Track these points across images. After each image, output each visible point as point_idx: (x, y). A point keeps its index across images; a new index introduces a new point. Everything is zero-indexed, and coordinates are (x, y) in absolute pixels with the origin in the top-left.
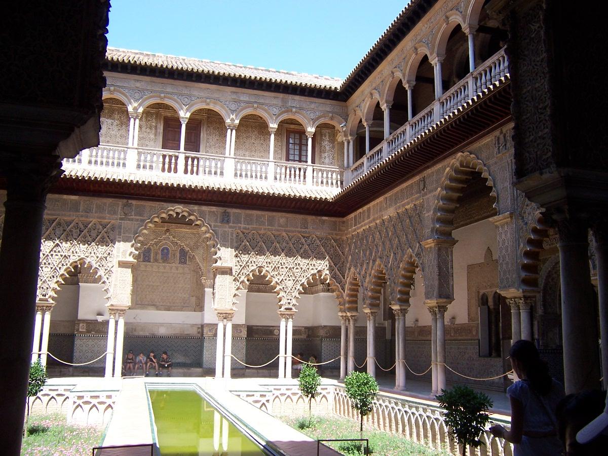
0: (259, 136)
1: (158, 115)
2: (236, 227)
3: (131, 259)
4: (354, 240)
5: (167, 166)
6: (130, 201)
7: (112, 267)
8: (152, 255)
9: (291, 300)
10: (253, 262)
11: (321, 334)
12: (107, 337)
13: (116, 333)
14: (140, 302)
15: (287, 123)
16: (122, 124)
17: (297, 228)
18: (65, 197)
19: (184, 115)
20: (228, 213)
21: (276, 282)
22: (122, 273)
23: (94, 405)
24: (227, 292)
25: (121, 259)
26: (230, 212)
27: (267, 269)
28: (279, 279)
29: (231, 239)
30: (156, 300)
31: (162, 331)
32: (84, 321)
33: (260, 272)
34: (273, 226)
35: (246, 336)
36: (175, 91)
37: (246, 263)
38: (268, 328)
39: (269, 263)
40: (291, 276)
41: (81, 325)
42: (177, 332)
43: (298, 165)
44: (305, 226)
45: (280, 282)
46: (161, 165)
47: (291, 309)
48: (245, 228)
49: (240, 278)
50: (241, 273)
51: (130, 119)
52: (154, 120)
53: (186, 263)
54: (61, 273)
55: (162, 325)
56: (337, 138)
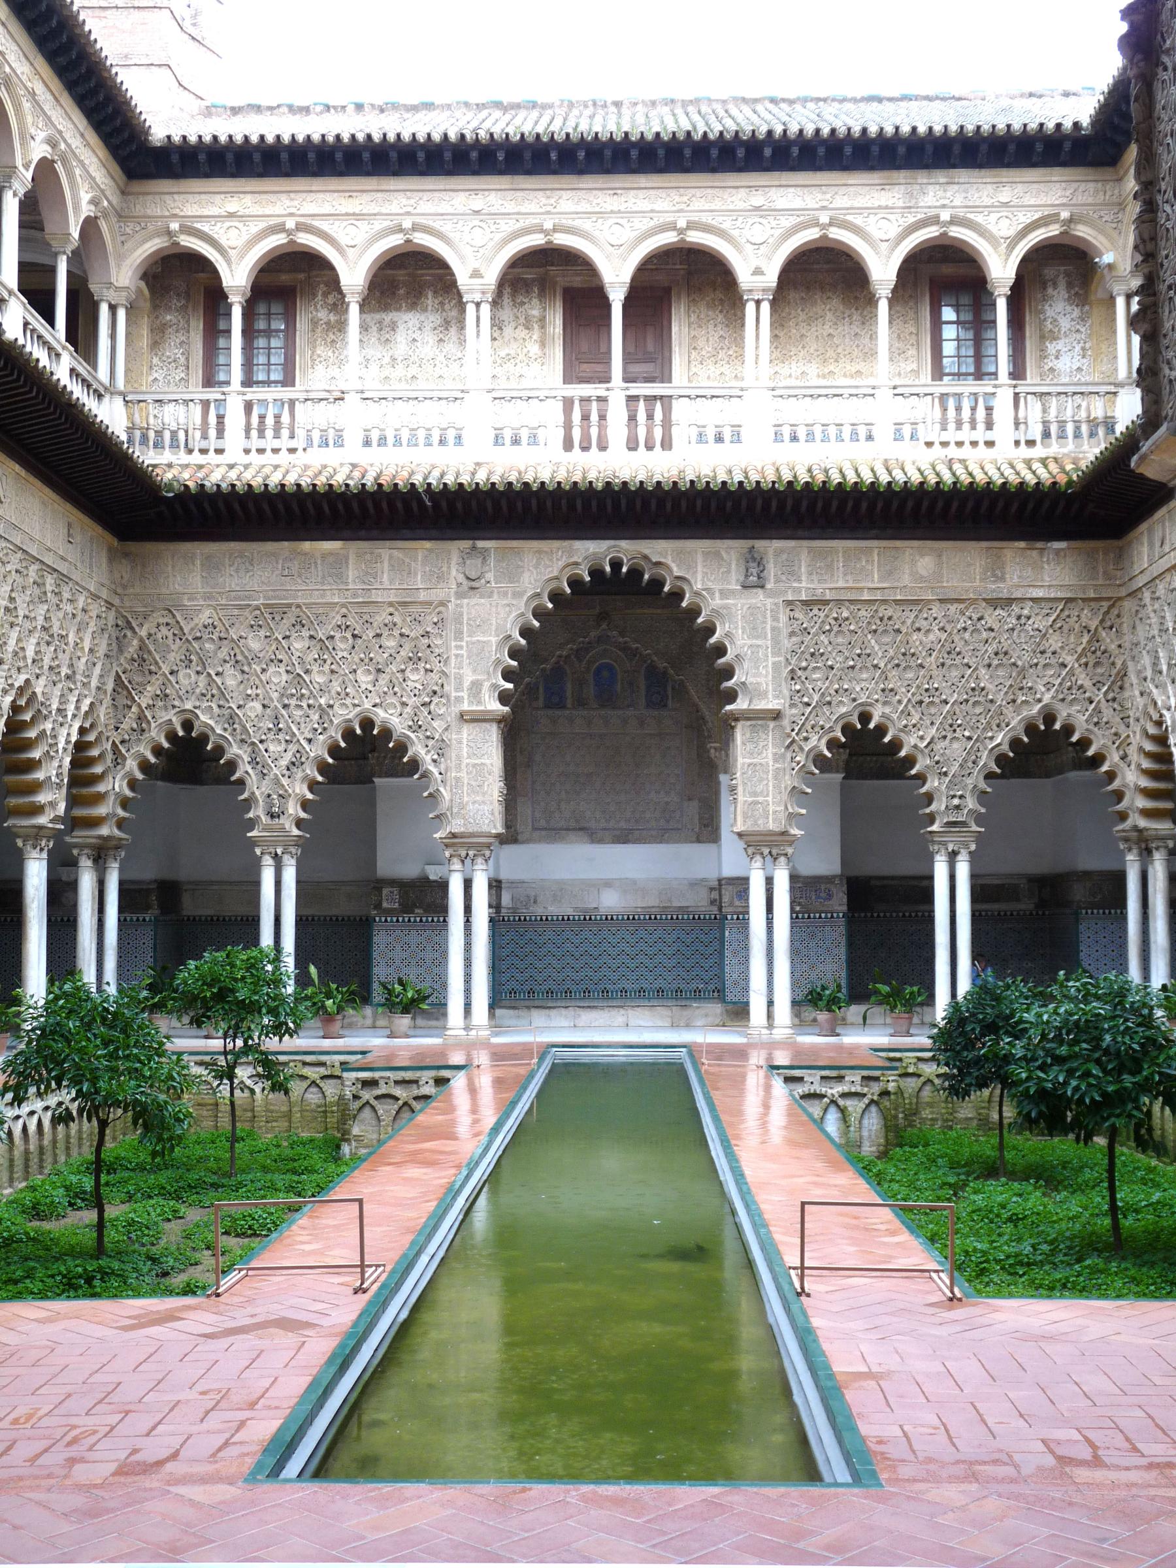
0: (847, 312)
1: (544, 287)
3: (494, 706)
5: (577, 434)
6: (480, 544)
7: (446, 729)
8: (569, 687)
11: (1078, 898)
12: (445, 921)
13: (468, 909)
14: (543, 823)
15: (930, 260)
16: (447, 324)
18: (307, 545)
19: (617, 277)
21: (915, 746)
22: (472, 744)
23: (405, 1104)
24: (771, 784)
25: (466, 707)
27: (887, 710)
29: (773, 629)
30: (588, 814)
31: (610, 902)
32: (392, 882)
33: (865, 717)
35: (845, 908)
36: (584, 207)
38: (915, 883)
41: (385, 891)
42: (652, 901)
43: (969, 387)
44: (994, 575)
46: (561, 432)
51: (461, 306)
52: (535, 301)
53: (665, 706)
54: (312, 755)
55: (608, 884)
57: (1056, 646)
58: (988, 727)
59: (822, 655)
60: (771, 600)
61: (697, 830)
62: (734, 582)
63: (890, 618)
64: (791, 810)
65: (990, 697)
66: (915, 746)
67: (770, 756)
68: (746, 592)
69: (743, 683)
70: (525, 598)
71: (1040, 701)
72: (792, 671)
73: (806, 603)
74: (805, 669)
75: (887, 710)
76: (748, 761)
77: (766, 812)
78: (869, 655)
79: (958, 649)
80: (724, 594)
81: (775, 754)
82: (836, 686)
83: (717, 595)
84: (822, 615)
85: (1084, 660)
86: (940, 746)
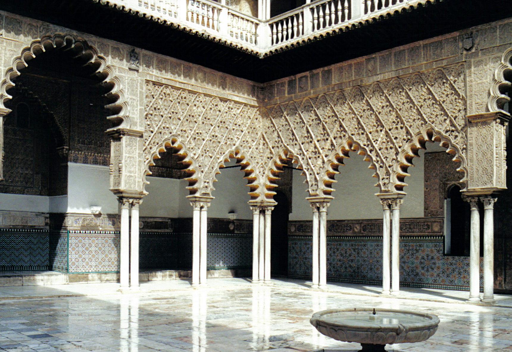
9: (208, 183)
28: (195, 154)
29: (140, 92)
40: (208, 151)
49: (151, 148)
50: (152, 142)
57: (240, 123)
58: (218, 154)
59: (159, 109)
60: (140, 78)
61: (40, 188)
62: (125, 65)
63: (185, 98)
65: (219, 140)
66: (193, 158)
67: (137, 154)
68: (131, 72)
69: (128, 117)
70: (22, 49)
71: (234, 145)
72: (147, 115)
73: (154, 83)
74: (152, 115)
76: (128, 155)
77: (135, 181)
78: (177, 113)
79: (208, 117)
80: (121, 70)
81: (139, 153)
82: (164, 125)
83: (117, 70)
84: (160, 90)
85: (248, 130)
86: (201, 158)
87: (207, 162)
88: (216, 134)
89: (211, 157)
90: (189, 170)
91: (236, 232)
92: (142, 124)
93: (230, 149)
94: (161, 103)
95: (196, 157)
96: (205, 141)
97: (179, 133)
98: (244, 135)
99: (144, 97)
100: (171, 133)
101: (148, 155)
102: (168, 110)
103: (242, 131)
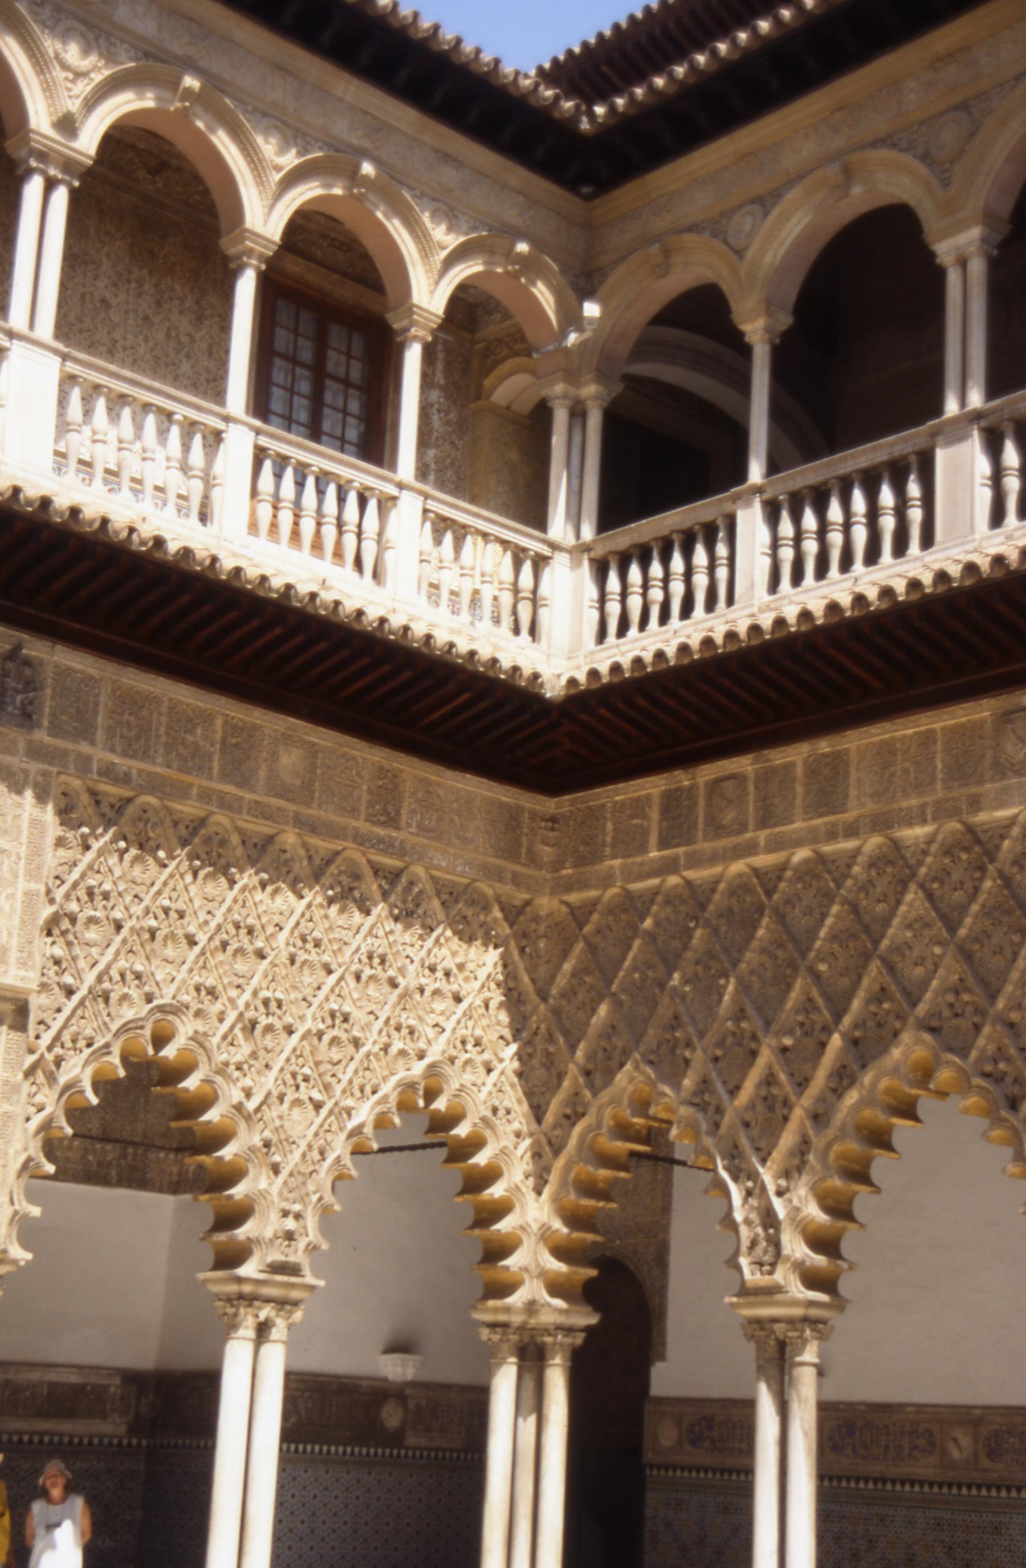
2: (65, 753)
4: (648, 923)
9: (298, 1216)
10: (129, 976)
17: (353, 812)
20: (27, 662)
21: (239, 1107)
26: (41, 663)
27: (200, 1026)
28: (248, 1094)
34: (244, 782)
37: (99, 979)
39: (212, 992)
40: (306, 1079)
43: (359, 474)
45: (258, 1110)
47: (293, 1270)
48: (108, 772)
49: (58, 1062)
50: (66, 1037)
56: (487, 382)
57: (450, 963)
59: (106, 896)
64: (17, 1207)
65: (356, 1033)
66: (239, 1107)
75: (200, 1026)
82: (122, 964)
87: (302, 1125)
88: (346, 1008)
89: (318, 1106)
90: (221, 1159)
91: (411, 1440)
92: (30, 955)
93: (401, 1074)
94: (118, 872)
95: (251, 1105)
96: (296, 1037)
97: (185, 998)
98: (468, 1015)
99: (50, 841)
100: (149, 998)
101: (46, 1090)
102: (147, 901)
103: (458, 999)
